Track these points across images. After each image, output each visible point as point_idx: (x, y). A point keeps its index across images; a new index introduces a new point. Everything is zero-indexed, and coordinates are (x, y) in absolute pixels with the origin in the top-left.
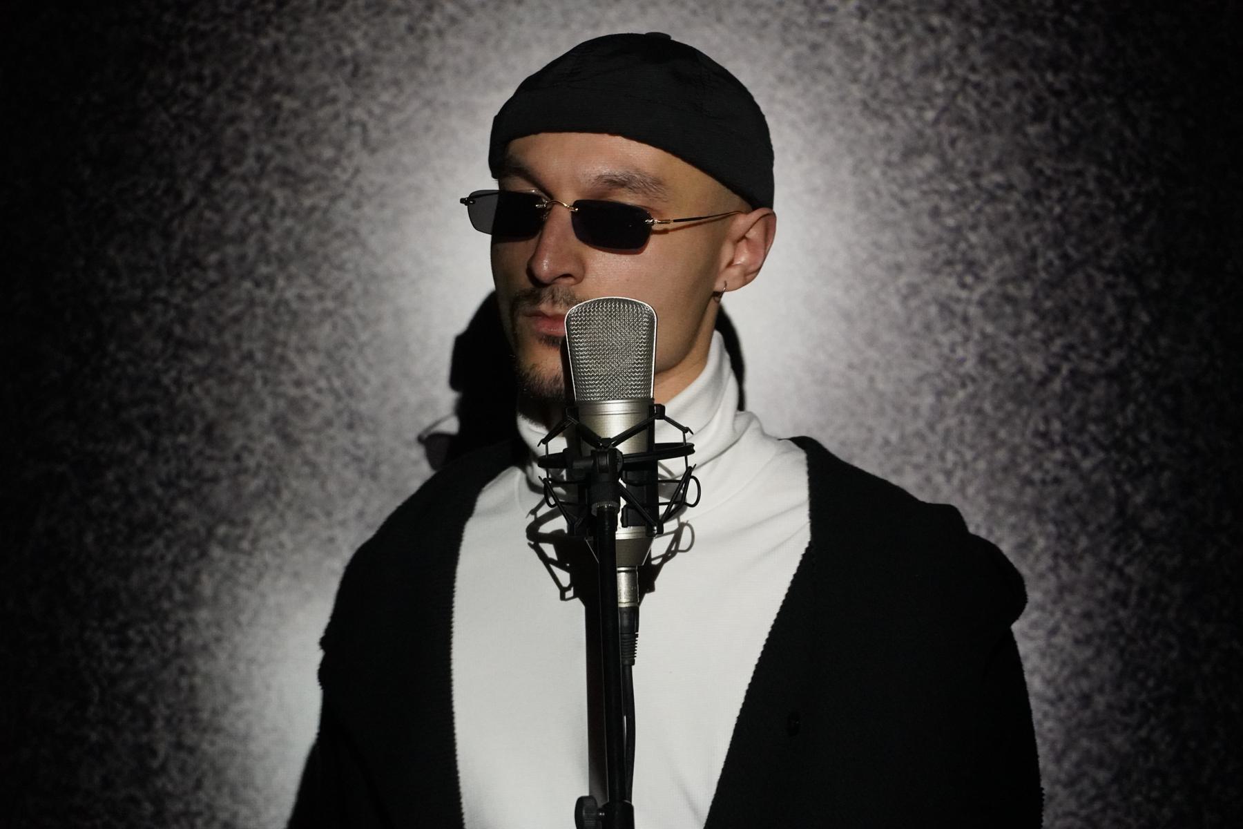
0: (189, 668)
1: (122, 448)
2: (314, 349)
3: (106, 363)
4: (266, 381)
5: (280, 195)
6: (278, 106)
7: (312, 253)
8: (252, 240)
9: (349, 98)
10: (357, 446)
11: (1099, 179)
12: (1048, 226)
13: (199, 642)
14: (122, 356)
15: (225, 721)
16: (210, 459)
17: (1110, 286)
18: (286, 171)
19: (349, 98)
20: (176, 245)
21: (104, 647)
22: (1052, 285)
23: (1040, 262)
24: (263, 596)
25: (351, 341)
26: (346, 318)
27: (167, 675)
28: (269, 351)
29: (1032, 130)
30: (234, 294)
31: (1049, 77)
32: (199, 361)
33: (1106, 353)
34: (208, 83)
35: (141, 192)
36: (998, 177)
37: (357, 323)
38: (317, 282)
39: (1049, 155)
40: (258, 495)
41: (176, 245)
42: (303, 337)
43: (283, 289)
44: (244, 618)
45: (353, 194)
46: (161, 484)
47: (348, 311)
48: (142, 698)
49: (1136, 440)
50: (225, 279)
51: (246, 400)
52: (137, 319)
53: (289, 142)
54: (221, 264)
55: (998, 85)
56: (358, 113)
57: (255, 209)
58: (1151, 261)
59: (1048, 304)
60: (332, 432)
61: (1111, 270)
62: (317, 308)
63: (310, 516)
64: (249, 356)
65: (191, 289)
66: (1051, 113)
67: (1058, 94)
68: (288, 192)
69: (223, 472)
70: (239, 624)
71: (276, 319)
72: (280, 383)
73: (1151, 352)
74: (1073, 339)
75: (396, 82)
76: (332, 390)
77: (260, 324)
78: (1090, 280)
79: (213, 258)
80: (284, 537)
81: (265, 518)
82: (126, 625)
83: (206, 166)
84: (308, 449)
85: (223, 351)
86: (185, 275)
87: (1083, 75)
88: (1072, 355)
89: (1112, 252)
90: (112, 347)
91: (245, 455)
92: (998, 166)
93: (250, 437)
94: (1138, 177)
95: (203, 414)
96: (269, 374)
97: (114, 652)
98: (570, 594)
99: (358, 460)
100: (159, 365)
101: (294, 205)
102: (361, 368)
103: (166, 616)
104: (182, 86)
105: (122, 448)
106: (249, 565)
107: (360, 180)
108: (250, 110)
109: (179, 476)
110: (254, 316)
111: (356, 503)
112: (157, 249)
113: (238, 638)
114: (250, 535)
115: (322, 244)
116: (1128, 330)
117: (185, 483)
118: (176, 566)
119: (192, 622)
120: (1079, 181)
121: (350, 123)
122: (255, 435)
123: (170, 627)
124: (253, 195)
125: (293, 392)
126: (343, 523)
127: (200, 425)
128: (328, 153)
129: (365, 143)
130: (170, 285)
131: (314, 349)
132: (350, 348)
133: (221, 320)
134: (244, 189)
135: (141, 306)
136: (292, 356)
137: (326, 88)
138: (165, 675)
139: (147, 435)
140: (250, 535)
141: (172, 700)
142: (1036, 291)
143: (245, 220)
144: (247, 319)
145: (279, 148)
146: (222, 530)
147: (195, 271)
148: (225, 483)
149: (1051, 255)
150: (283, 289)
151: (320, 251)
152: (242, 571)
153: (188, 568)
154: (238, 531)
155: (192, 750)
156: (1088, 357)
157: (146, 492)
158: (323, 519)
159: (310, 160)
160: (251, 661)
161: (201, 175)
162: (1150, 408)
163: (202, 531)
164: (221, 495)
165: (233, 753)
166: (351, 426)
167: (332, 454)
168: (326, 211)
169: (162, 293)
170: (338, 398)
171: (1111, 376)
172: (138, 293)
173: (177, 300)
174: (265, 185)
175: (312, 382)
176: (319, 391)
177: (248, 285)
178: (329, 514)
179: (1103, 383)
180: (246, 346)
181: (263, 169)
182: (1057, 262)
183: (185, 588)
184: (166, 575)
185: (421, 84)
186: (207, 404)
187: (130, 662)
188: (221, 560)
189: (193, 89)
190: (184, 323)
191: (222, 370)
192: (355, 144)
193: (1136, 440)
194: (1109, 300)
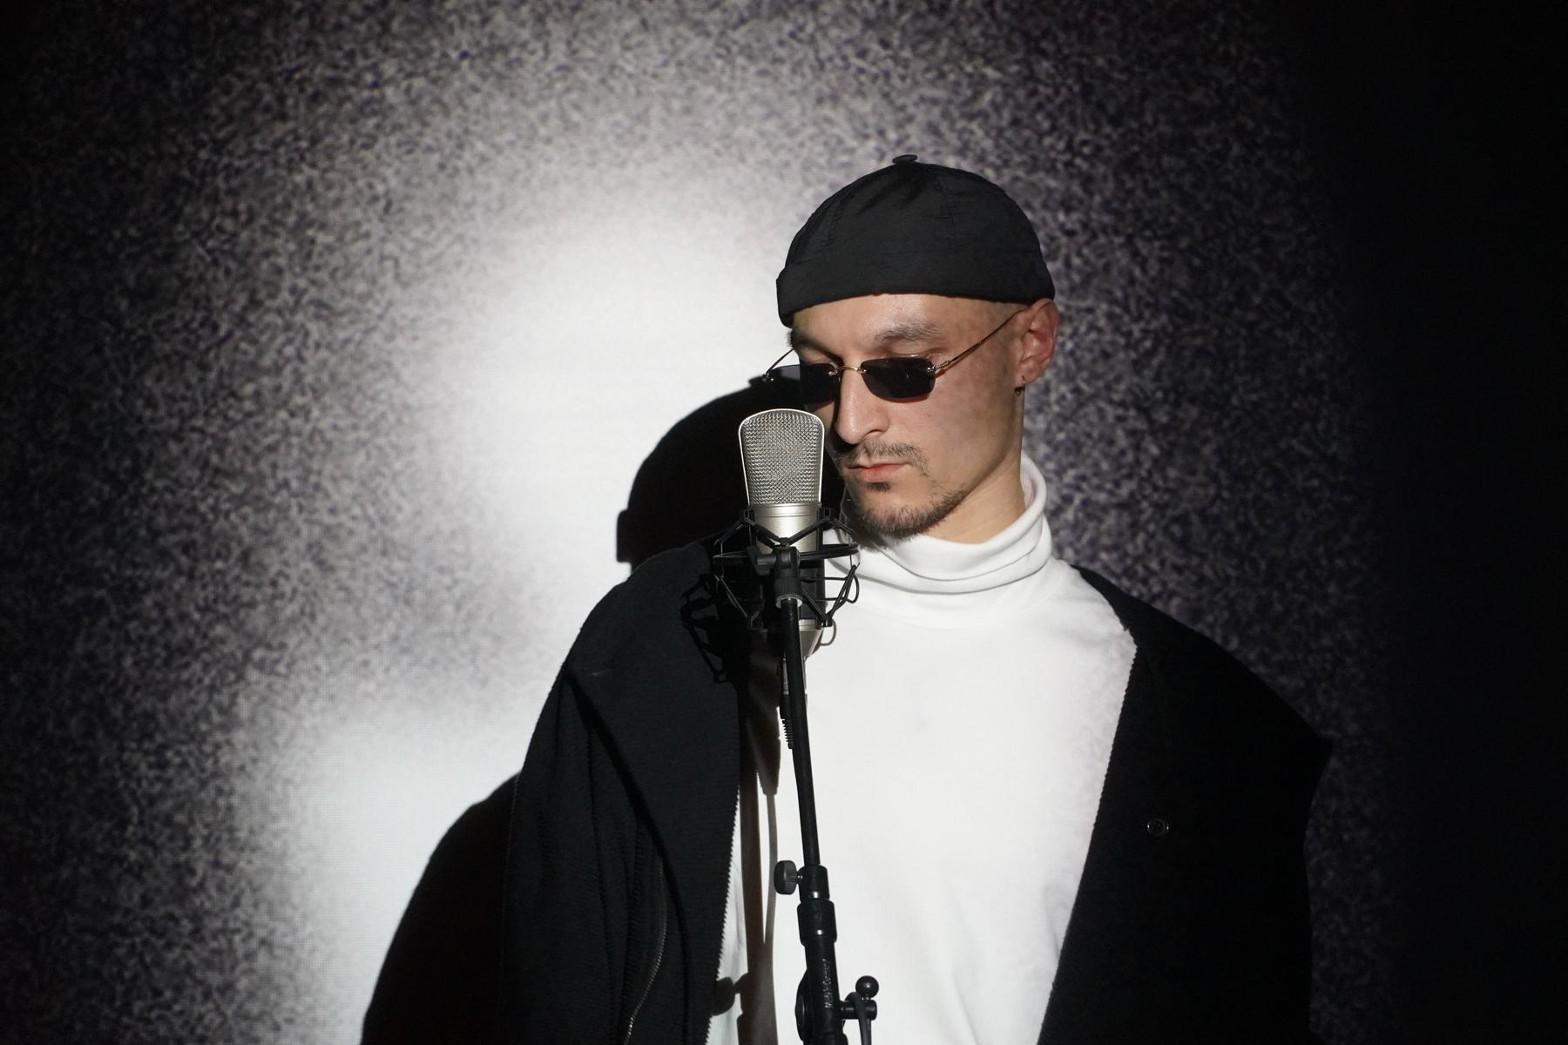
0: (226, 788)
1: (160, 574)
2: (349, 477)
3: (144, 490)
4: (301, 509)
5: (314, 328)
6: (313, 241)
7: (345, 384)
8: (288, 370)
9: (382, 233)
10: (392, 573)
11: (1110, 316)
12: (1061, 361)
13: (237, 764)
14: (160, 484)
15: (263, 839)
16: (247, 584)
17: (1120, 419)
18: (320, 304)
19: (382, 233)
20: (212, 376)
21: (143, 767)
22: (1065, 418)
23: (1053, 396)
24: (299, 718)
25: (385, 470)
26: (380, 448)
27: (207, 795)
28: (304, 479)
30: (270, 424)
31: (1061, 217)
32: (236, 489)
33: (1117, 484)
34: (243, 218)
35: (178, 324)
38: (349, 410)
40: (292, 621)
41: (212, 376)
42: (338, 467)
43: (318, 420)
44: (280, 740)
45: (384, 326)
46: (199, 609)
47: (381, 441)
48: (180, 818)
49: (1146, 567)
50: (261, 410)
51: (281, 527)
52: (174, 448)
53: (323, 275)
54: (257, 394)
56: (390, 248)
57: (290, 341)
58: (1159, 395)
59: (1061, 436)
60: (365, 558)
61: (1122, 404)
62: (351, 436)
63: (345, 640)
64: (286, 484)
65: (226, 418)
66: (1064, 251)
67: (1070, 234)
68: (323, 324)
69: (259, 597)
70: (275, 744)
71: (311, 449)
72: (315, 511)
73: (1160, 483)
74: (1082, 470)
75: (428, 218)
76: (367, 518)
77: (295, 452)
78: (1101, 413)
79: (249, 389)
80: (320, 661)
81: (301, 643)
82: (164, 747)
83: (242, 300)
84: (344, 575)
85: (260, 479)
86: (221, 405)
87: (1094, 216)
88: (1084, 486)
89: (1122, 387)
90: (149, 476)
91: (282, 581)
93: (286, 563)
94: (1147, 314)
95: (240, 542)
96: (304, 502)
97: (152, 773)
98: (722, 678)
99: (392, 585)
100: (196, 492)
101: (329, 338)
102: (394, 495)
103: (203, 738)
104: (217, 221)
105: (160, 574)
106: (285, 687)
107: (393, 313)
108: (285, 245)
109: (215, 601)
110: (289, 446)
111: (391, 627)
112: (194, 380)
113: (274, 759)
114: (287, 659)
115: (356, 376)
116: (1138, 463)
117: (222, 608)
118: (213, 689)
119: (229, 742)
120: (1090, 317)
121: (383, 258)
122: (288, 560)
123: (208, 748)
124: (288, 327)
125: (328, 520)
126: (377, 647)
127: (236, 552)
128: (361, 287)
129: (397, 276)
130: (207, 414)
131: (349, 477)
132: (384, 476)
133: (257, 449)
134: (279, 321)
135: (178, 436)
136: (327, 484)
137: (358, 224)
138: (203, 795)
139: (184, 560)
140: (287, 659)
141: (209, 819)
142: (1049, 424)
143: (280, 352)
144: (282, 448)
145: (313, 282)
146: (258, 654)
147: (231, 401)
148: (262, 608)
149: (1063, 389)
150: (318, 420)
151: (354, 383)
152: (278, 694)
153: (225, 690)
154: (275, 655)
155: (229, 869)
156: (1099, 488)
157: (183, 617)
158: (357, 642)
159: (343, 293)
160: (288, 781)
161: (237, 308)
162: (1160, 538)
163: (239, 655)
164: (258, 619)
165: (270, 871)
166: (384, 553)
167: (366, 578)
168: (360, 343)
169: (199, 422)
170: (372, 525)
171: (1122, 506)
172: (175, 422)
173: (212, 429)
174: (299, 318)
175: (347, 510)
176: (354, 518)
177: (283, 414)
178: (363, 638)
179: (1113, 513)
180: (281, 475)
181: (297, 303)
182: (1069, 396)
183: (223, 711)
184: (203, 697)
185: (453, 221)
186: (243, 530)
187: (169, 782)
188: (258, 683)
189: (229, 224)
190: (220, 452)
191: (259, 498)
192: (388, 278)
193: (1146, 567)
194: (1120, 433)
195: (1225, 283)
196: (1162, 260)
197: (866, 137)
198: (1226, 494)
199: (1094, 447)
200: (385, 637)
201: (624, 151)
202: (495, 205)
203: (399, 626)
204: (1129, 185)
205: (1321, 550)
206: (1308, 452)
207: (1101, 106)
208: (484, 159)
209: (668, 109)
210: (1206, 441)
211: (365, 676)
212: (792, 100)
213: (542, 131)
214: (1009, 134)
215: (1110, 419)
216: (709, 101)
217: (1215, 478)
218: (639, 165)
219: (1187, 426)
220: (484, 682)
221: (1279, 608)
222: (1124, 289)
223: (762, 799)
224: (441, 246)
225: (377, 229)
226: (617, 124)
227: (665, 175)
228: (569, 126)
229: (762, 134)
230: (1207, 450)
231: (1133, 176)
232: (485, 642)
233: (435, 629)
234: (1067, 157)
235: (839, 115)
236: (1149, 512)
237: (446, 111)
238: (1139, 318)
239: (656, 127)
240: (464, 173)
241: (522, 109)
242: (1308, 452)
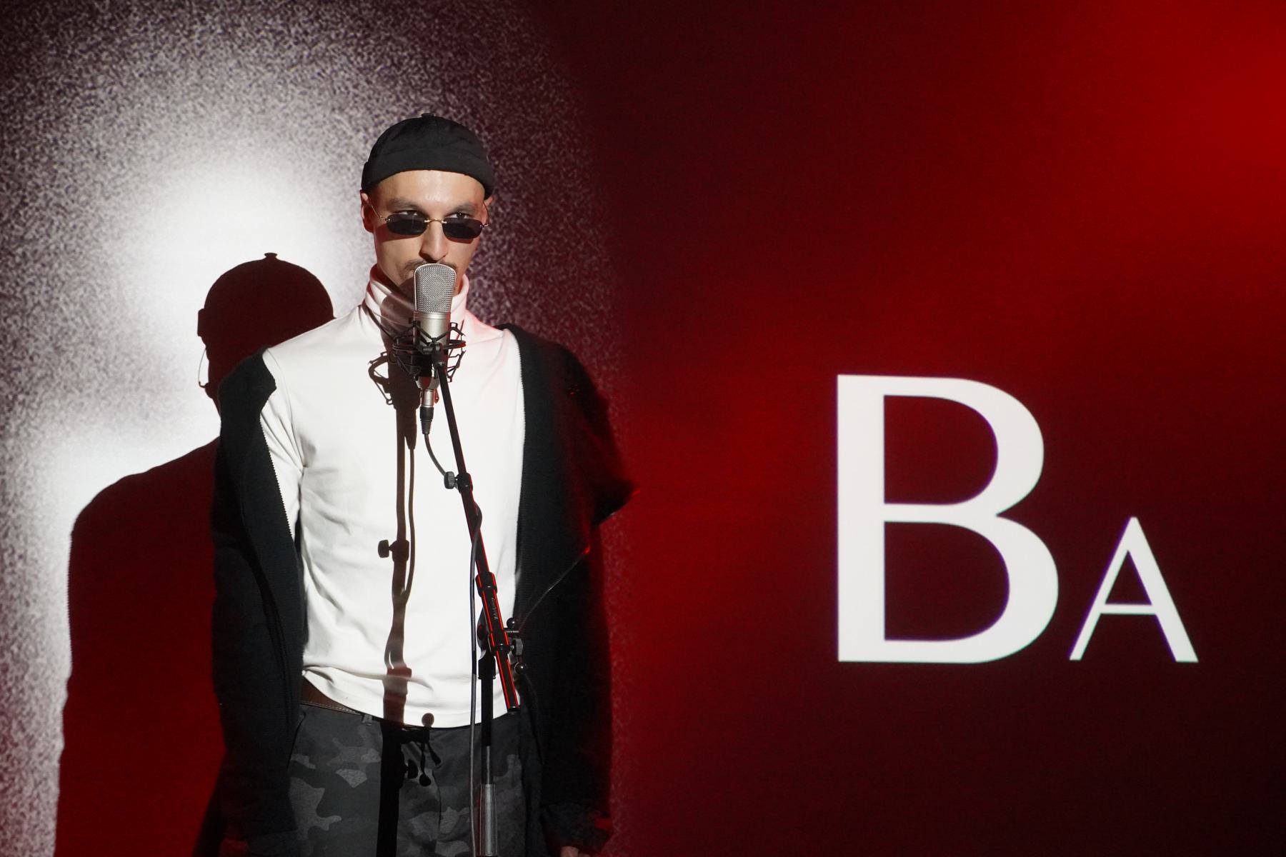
17: (490, 287)
37: (98, 289)
56: (99, 177)
60: (82, 346)
78: (480, 284)
99: (96, 361)
102: (99, 312)
111: (96, 384)
126: (89, 395)
128: (83, 198)
129: (102, 193)
166: (93, 344)
192: (98, 194)
196: (512, 203)
197: (358, 131)
200: (92, 391)
201: (228, 132)
202: (157, 158)
203: (101, 385)
205: (594, 360)
206: (589, 308)
207: (482, 121)
208: (151, 131)
210: (535, 300)
211: (78, 412)
212: (318, 109)
213: (184, 119)
216: (274, 107)
217: (540, 321)
220: (147, 417)
224: (127, 178)
225: (93, 167)
226: (223, 117)
227: (250, 145)
229: (301, 125)
230: (535, 305)
231: (498, 159)
232: (147, 395)
233: (119, 386)
235: (343, 118)
237: (132, 105)
238: (501, 233)
240: (140, 138)
242: (589, 308)
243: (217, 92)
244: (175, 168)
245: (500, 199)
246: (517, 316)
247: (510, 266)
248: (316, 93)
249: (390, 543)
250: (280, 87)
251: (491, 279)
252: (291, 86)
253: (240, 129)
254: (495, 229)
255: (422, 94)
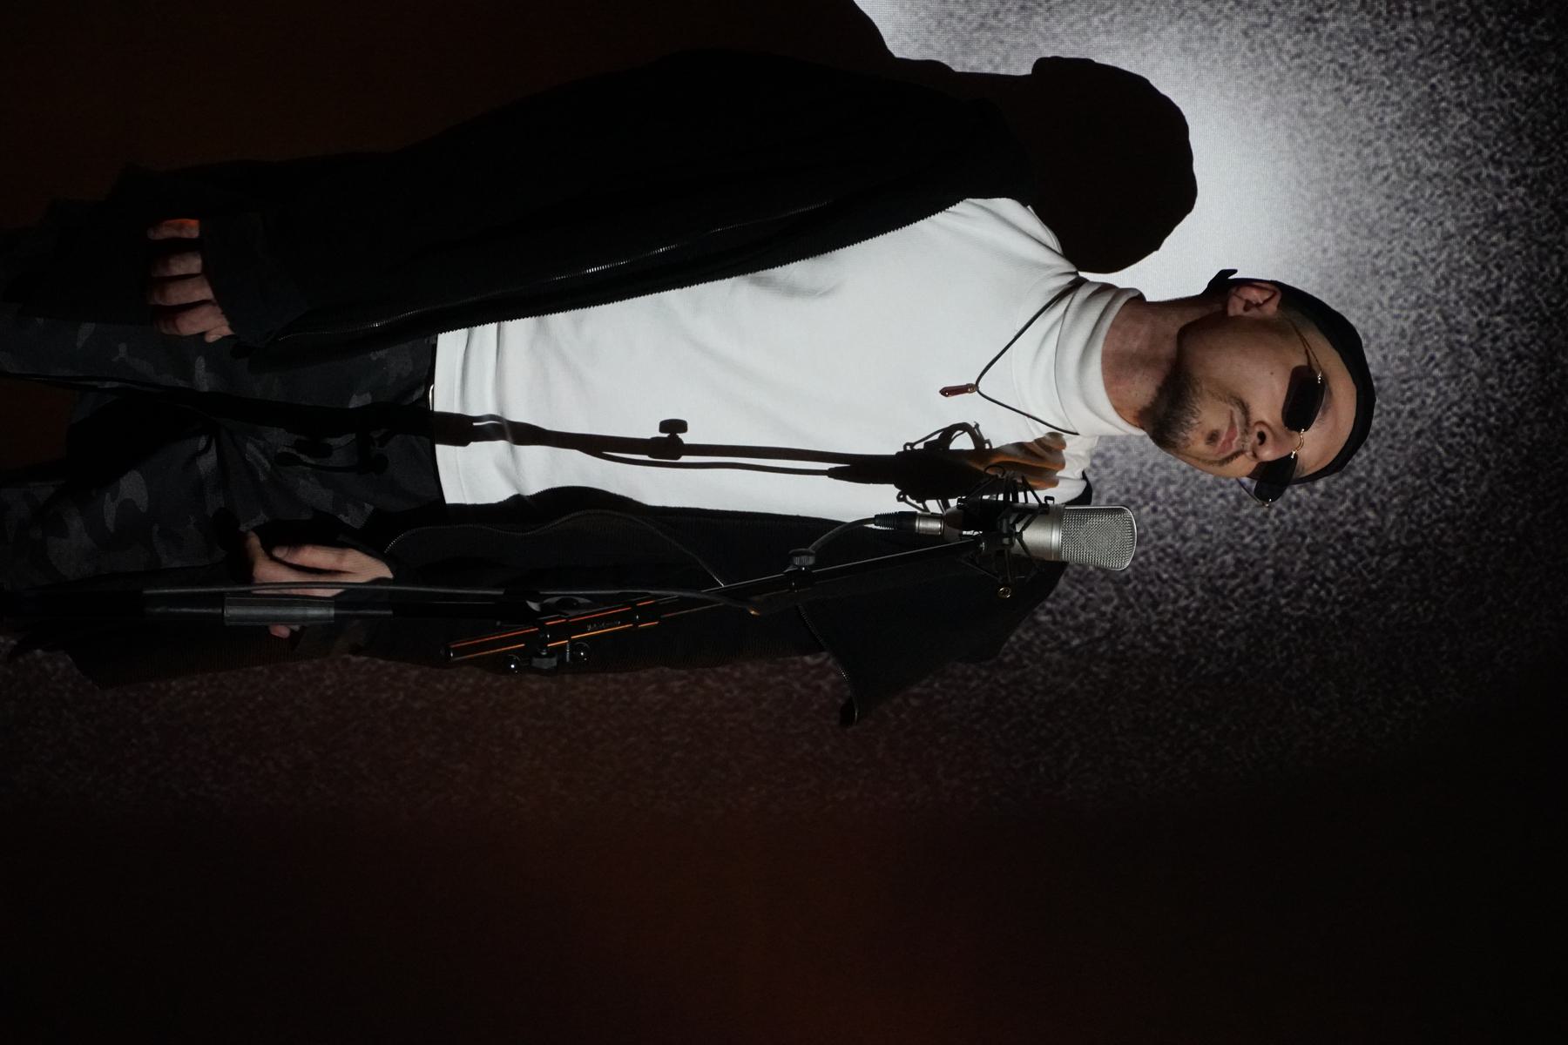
11: (1186, 609)
17: (1104, 614)
29: (1229, 558)
31: (1270, 571)
33: (1049, 612)
36: (1193, 528)
39: (1208, 570)
55: (1265, 532)
58: (1121, 647)
67: (1256, 579)
78: (1107, 601)
92: (1202, 530)
195: (1207, 703)
196: (1231, 650)
198: (1037, 698)
199: (1081, 592)
201: (1346, 217)
202: (1307, 109)
204: (1293, 628)
208: (1347, 101)
209: (1376, 256)
213: (1366, 151)
214: (1341, 531)
215: (1103, 608)
216: (1382, 288)
218: (1333, 230)
219: (1095, 669)
221: (943, 739)
222: (1208, 621)
223: (826, 466)
227: (1325, 251)
228: (1370, 173)
230: (1073, 685)
231: (1298, 630)
234: (1319, 578)
236: (1026, 637)
238: (1184, 633)
239: (1362, 245)
241: (1385, 135)
243: (1406, 202)
244: (1291, 136)
245: (1238, 631)
246: (1056, 656)
247: (1133, 646)
248: (1404, 352)
249: (680, 436)
250: (1413, 298)
251: (1115, 617)
252: (1414, 315)
253: (1349, 236)
254: (1191, 623)
255: (1400, 515)
